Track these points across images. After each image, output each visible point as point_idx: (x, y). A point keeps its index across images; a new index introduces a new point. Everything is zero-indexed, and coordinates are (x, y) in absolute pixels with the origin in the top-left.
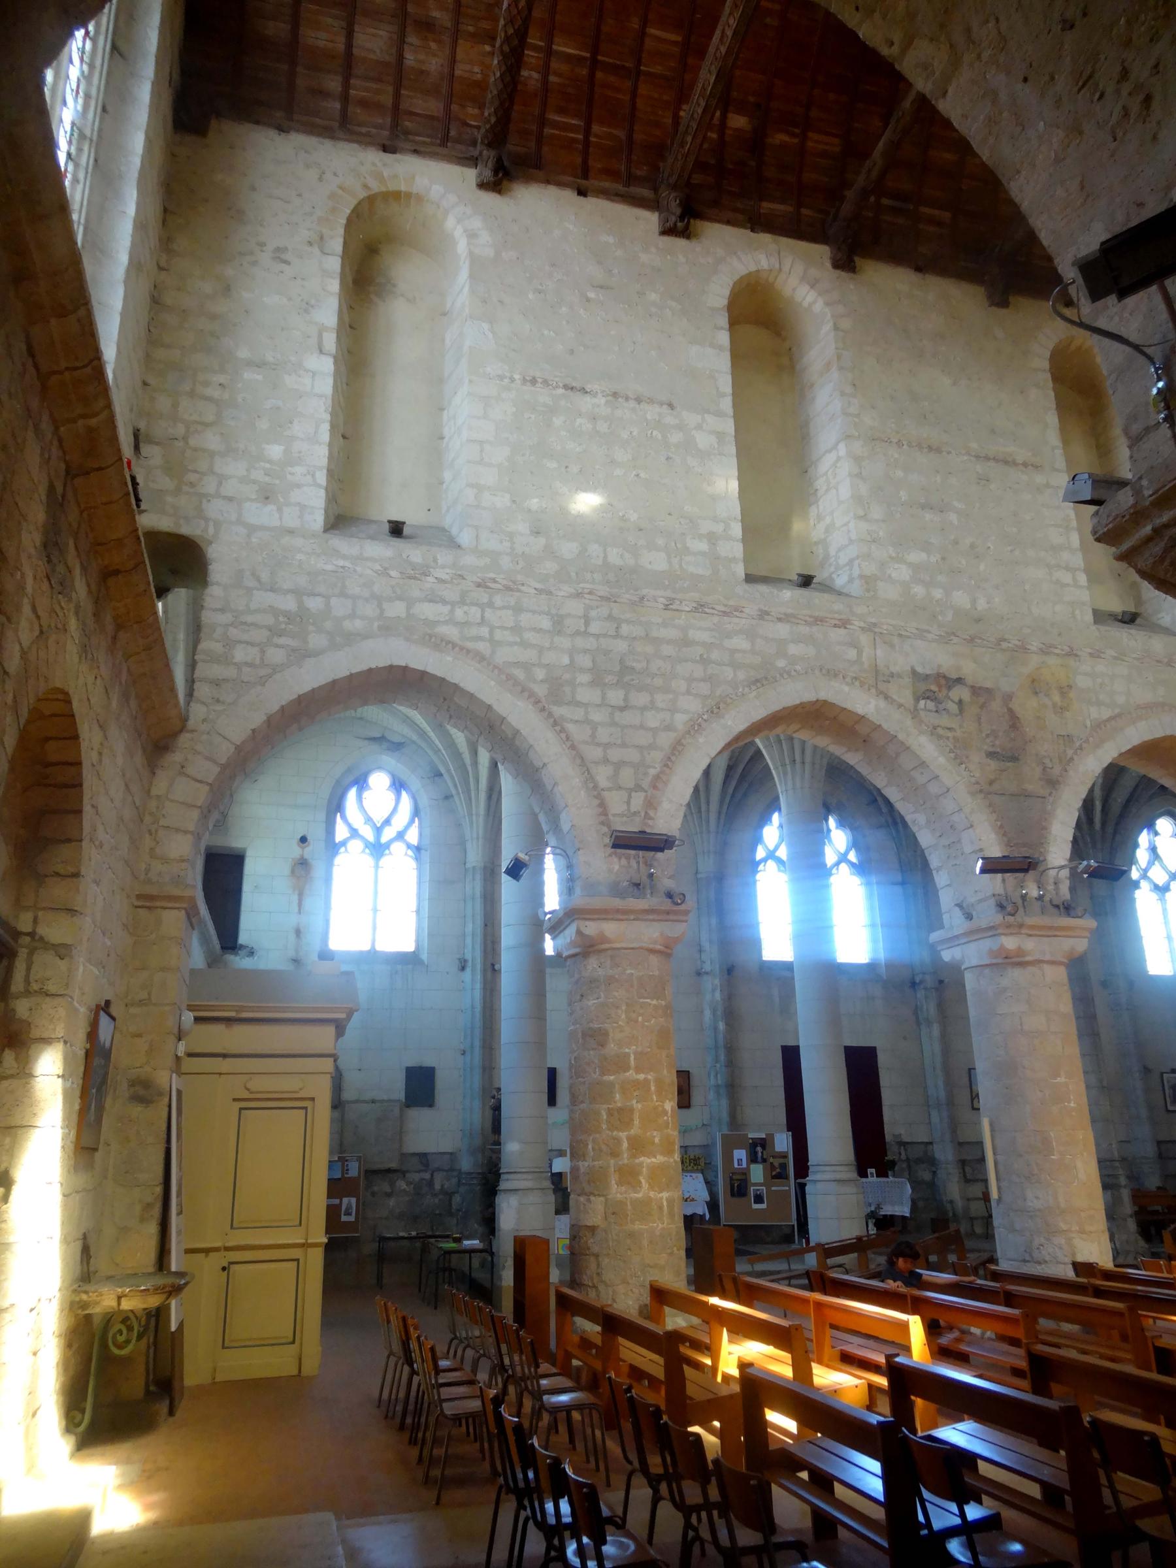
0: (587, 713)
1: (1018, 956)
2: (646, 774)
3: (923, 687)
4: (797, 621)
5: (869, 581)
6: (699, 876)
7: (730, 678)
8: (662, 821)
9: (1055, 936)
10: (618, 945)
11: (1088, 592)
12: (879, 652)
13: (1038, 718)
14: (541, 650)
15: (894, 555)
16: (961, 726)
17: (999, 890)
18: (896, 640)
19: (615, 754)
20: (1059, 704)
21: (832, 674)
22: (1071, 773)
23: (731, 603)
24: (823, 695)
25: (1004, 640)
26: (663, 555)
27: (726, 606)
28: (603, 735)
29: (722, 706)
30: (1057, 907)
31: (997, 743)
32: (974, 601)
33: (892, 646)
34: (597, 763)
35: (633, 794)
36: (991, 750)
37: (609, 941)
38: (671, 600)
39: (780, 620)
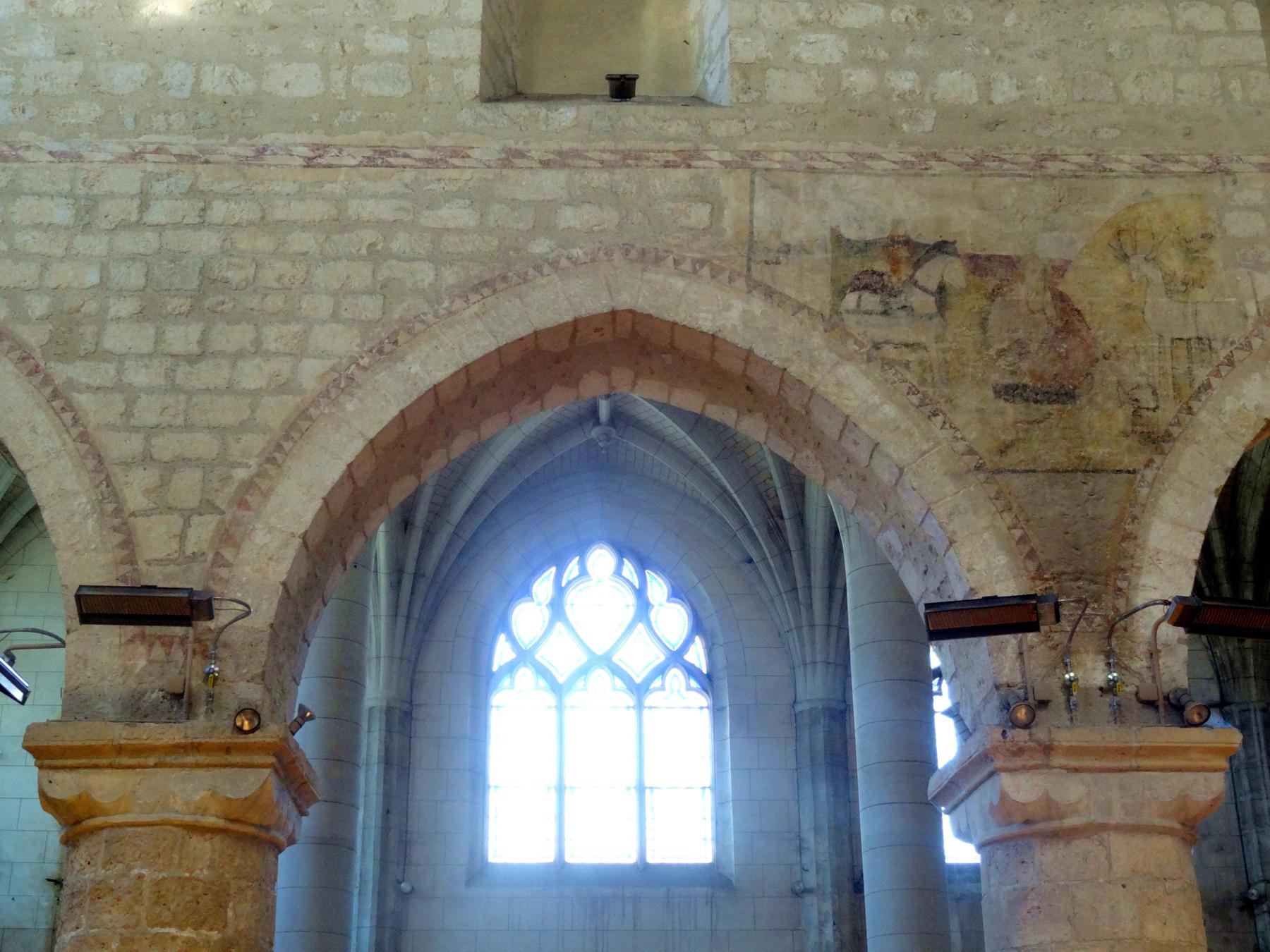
0: (120, 372)
1: (1049, 818)
2: (226, 480)
3: (855, 265)
4: (582, 163)
5: (746, 71)
6: (799, 708)
7: (426, 284)
8: (247, 569)
9: (1138, 769)
10: (117, 819)
11: (1261, 42)
12: (760, 207)
13: (1128, 307)
14: (45, 263)
15: (809, 17)
16: (939, 338)
17: (1009, 671)
18: (801, 181)
19: (165, 447)
20: (1180, 274)
21: (649, 258)
22: (1203, 416)
23: (446, 142)
24: (624, 300)
25: (1055, 157)
26: (315, 68)
27: (433, 149)
28: (147, 412)
29: (401, 339)
30: (1150, 704)
31: (1025, 365)
32: (986, 87)
33: (791, 191)
34: (127, 465)
35: (196, 519)
36: (1009, 380)
37: (105, 812)
38: (321, 149)
39: (546, 164)
